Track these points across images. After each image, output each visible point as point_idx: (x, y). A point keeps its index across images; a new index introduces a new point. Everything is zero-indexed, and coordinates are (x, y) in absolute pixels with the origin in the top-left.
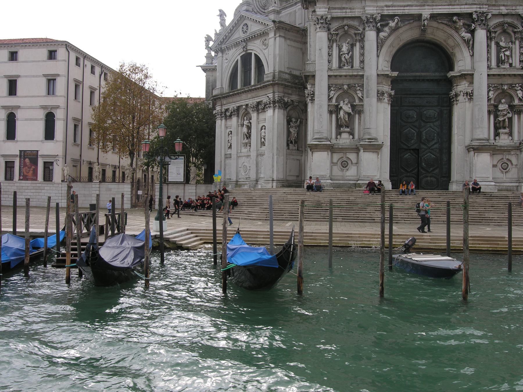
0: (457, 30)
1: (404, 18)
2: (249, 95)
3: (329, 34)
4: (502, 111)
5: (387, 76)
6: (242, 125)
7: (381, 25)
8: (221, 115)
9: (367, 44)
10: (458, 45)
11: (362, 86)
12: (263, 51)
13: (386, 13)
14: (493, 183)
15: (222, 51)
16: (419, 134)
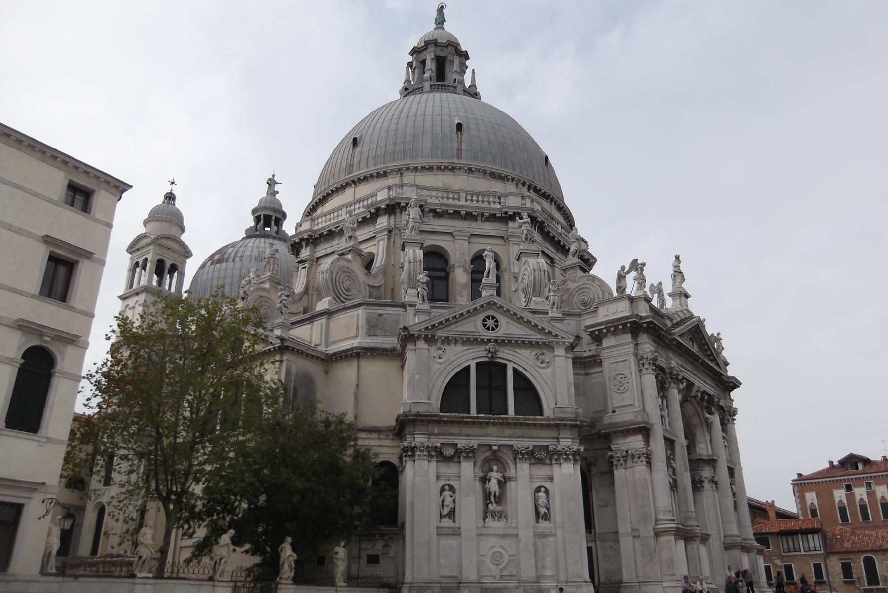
2: (508, 431)
6: (485, 480)
8: (429, 452)
12: (539, 370)
15: (430, 340)
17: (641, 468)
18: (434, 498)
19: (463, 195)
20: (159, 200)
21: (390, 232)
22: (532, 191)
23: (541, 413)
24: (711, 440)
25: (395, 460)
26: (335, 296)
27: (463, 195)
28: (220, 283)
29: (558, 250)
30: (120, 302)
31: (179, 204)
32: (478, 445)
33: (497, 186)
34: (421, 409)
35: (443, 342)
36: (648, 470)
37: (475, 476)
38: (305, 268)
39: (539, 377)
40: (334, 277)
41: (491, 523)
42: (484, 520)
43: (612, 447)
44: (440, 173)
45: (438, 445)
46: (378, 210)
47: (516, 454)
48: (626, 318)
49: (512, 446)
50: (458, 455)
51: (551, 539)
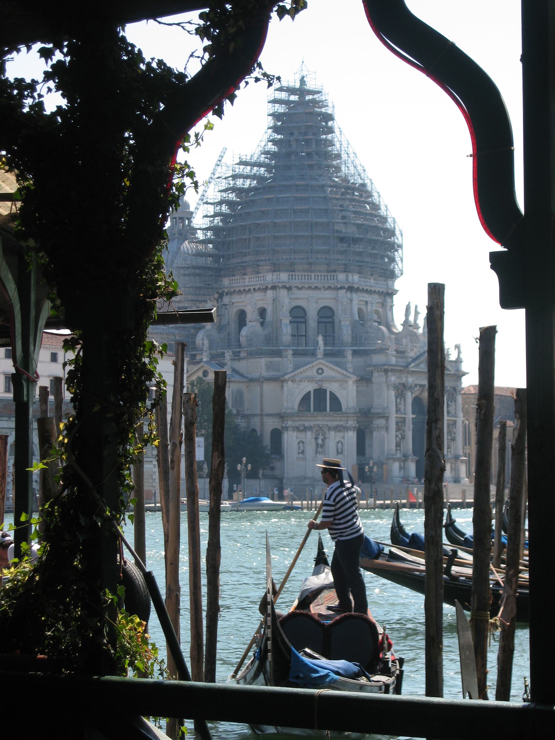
2: (326, 419)
6: (316, 438)
11: (405, 424)
17: (383, 432)
18: (295, 446)
21: (274, 300)
25: (280, 428)
29: (371, 294)
32: (314, 425)
35: (299, 381)
36: (385, 434)
38: (227, 309)
39: (341, 395)
42: (316, 454)
43: (374, 423)
45: (297, 425)
47: (330, 428)
49: (327, 425)
50: (305, 429)
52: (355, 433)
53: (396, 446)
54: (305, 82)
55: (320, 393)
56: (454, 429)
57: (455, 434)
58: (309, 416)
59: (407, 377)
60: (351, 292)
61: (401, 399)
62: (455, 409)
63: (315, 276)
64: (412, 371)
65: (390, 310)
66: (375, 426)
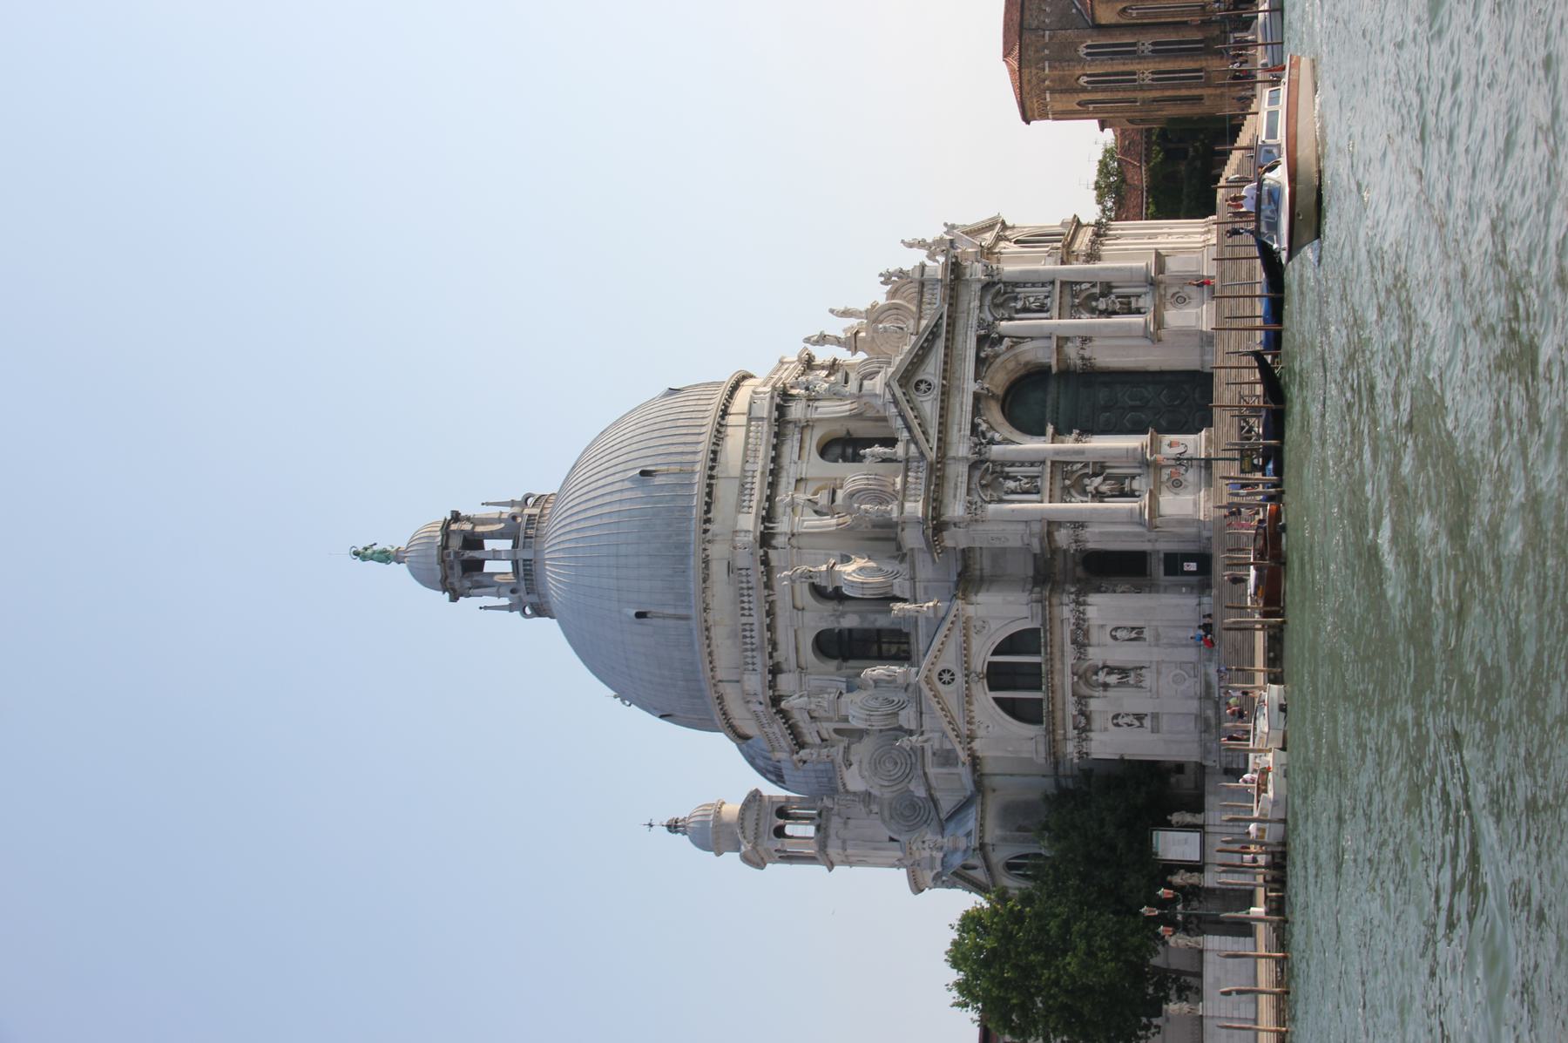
0: (997, 356)
1: (976, 411)
2: (1058, 665)
3: (990, 502)
4: (1107, 305)
5: (1053, 436)
6: (1106, 686)
7: (984, 438)
9: (1009, 458)
10: (1016, 356)
11: (1067, 463)
13: (968, 433)
14: (1205, 306)
15: (971, 738)
16: (1133, 408)
19: (744, 620)
20: (682, 840)
22: (709, 516)
23: (1037, 631)
24: (1032, 338)
26: (907, 780)
27: (744, 620)
28: (813, 774)
29: (781, 468)
30: (836, 868)
31: (681, 814)
33: (718, 570)
34: (1042, 748)
37: (1105, 697)
40: (886, 784)
41: (1147, 683)
43: (1065, 547)
44: (713, 641)
46: (775, 713)
48: (927, 540)
51: (1160, 630)
52: (1093, 598)
53: (1122, 494)
54: (366, 549)
55: (998, 677)
56: (1083, 286)
57: (1094, 285)
58: (1053, 705)
59: (954, 458)
60: (773, 536)
61: (1008, 477)
62: (1034, 285)
63: (743, 615)
64: (939, 448)
65: (817, 408)
66: (1074, 546)
